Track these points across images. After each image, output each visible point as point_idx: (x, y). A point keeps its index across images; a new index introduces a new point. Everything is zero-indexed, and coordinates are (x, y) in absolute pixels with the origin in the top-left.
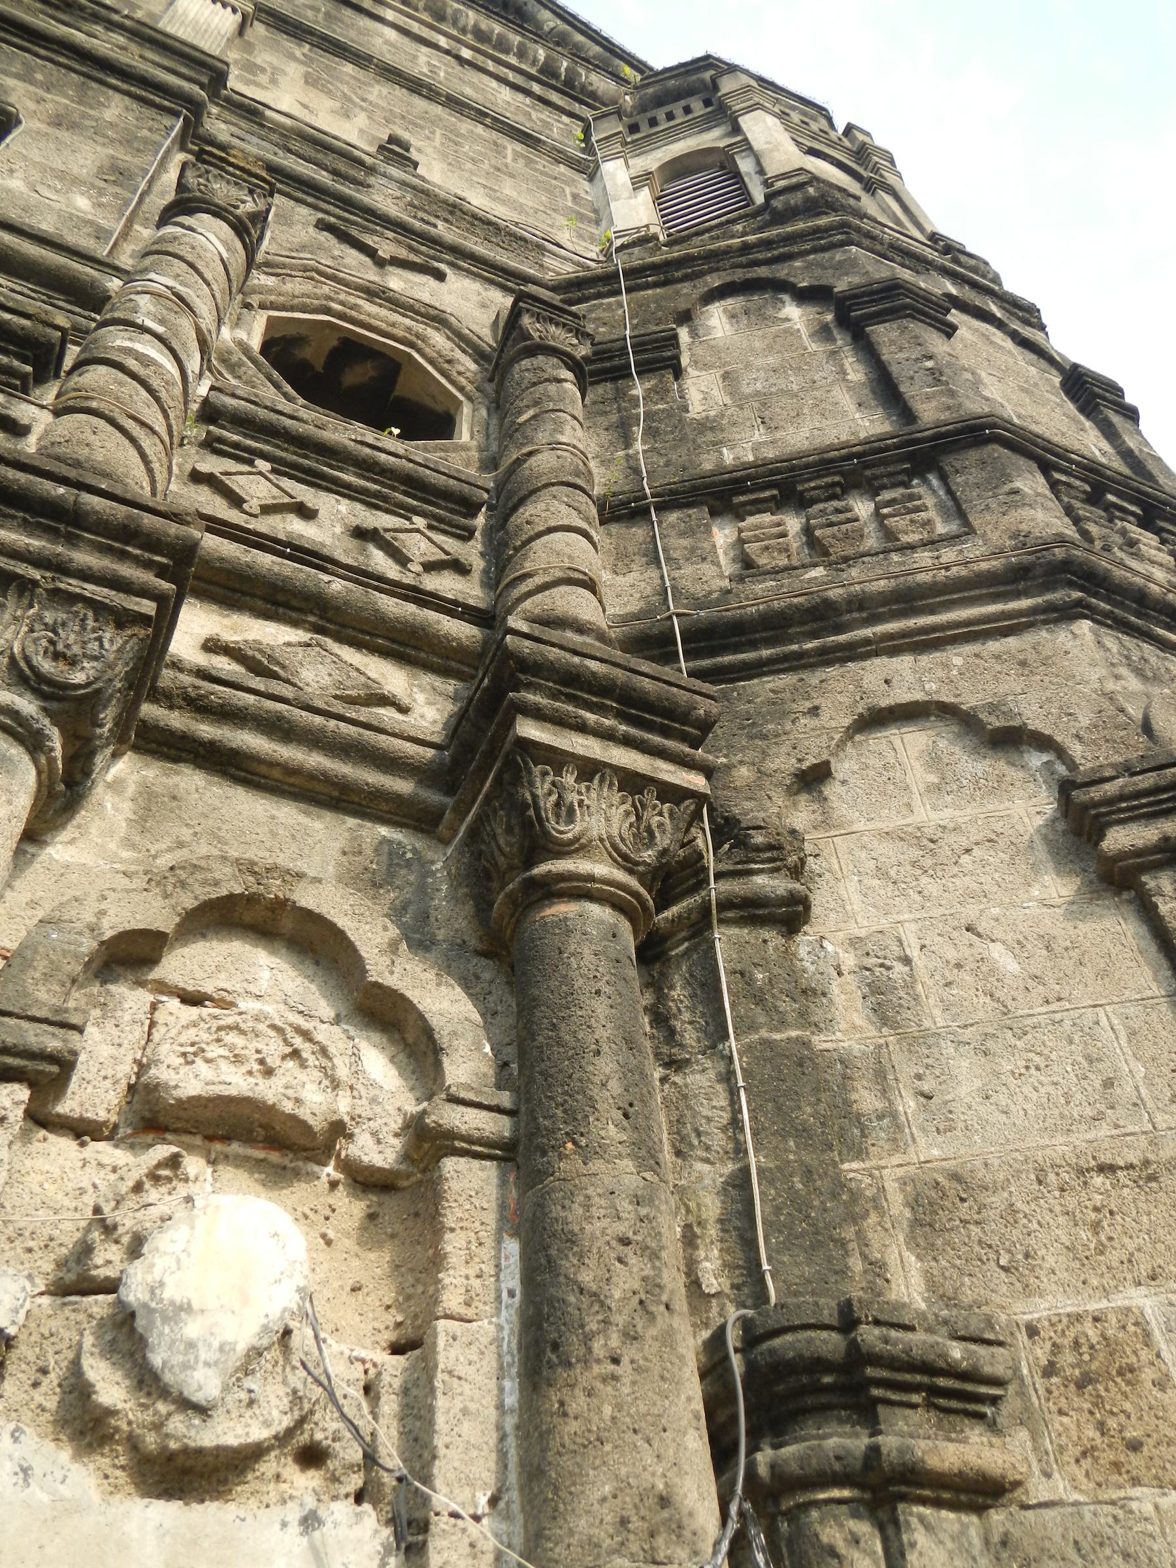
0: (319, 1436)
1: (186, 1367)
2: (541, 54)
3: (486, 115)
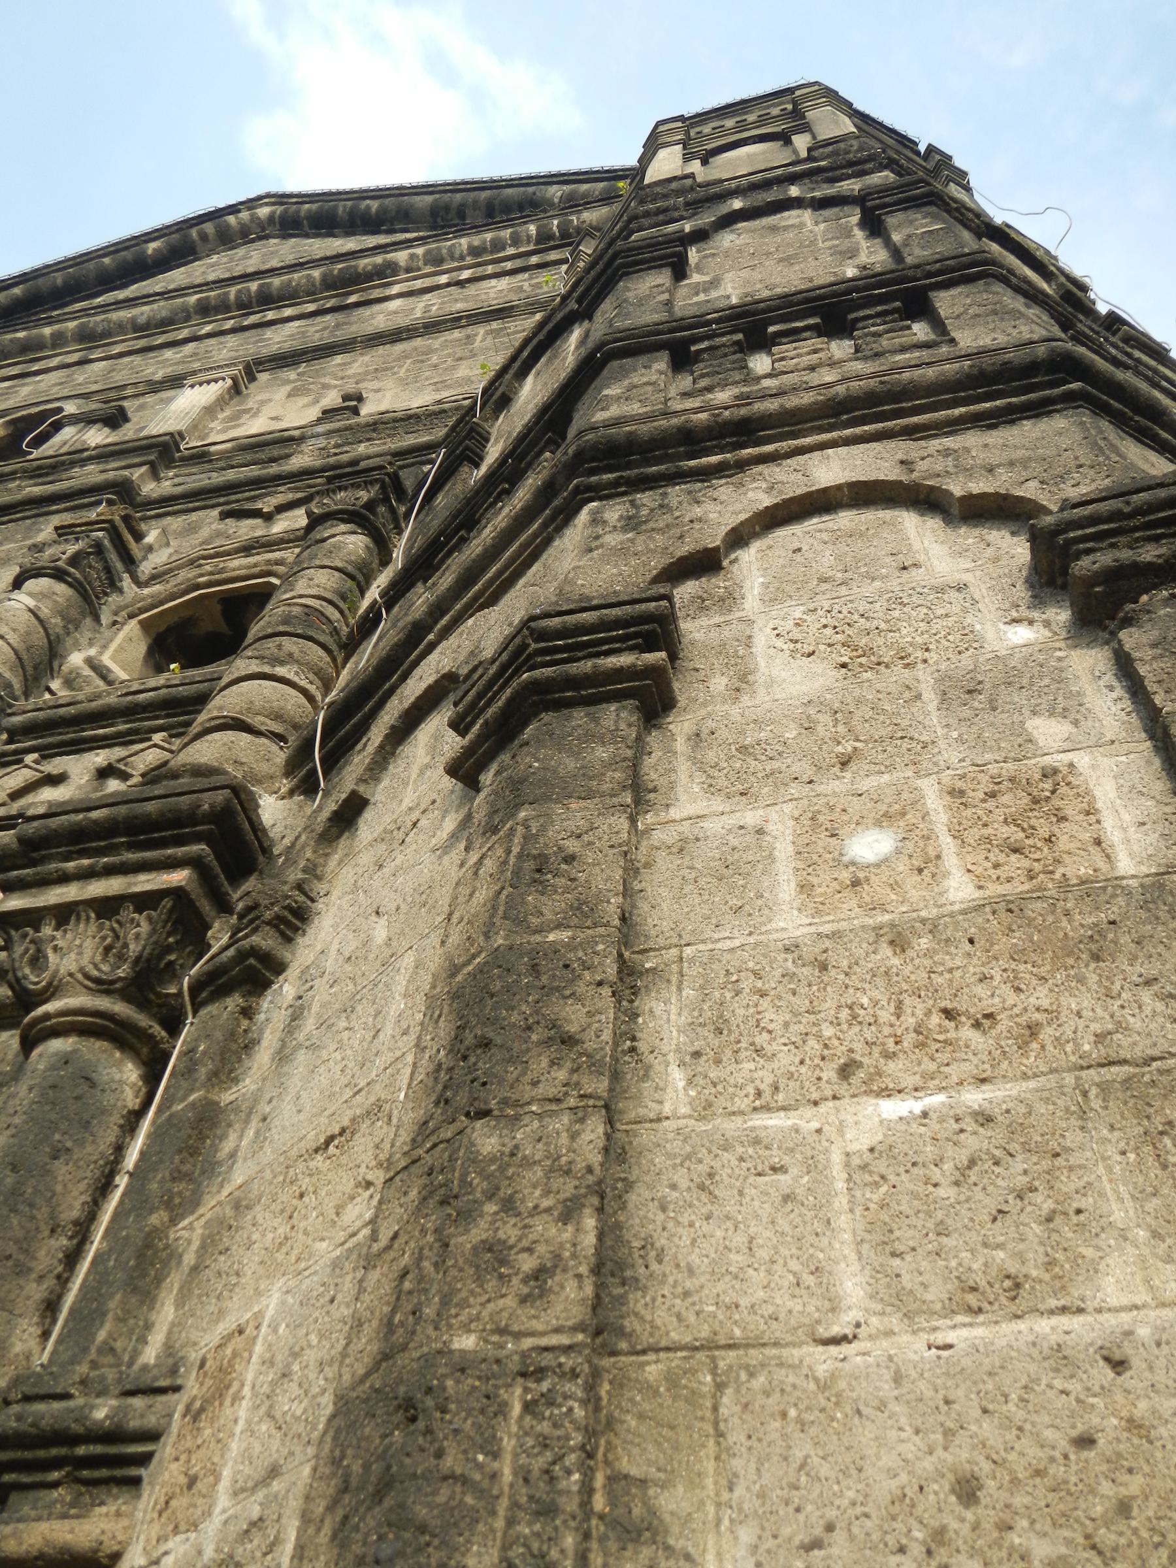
2: (532, 229)
3: (460, 318)
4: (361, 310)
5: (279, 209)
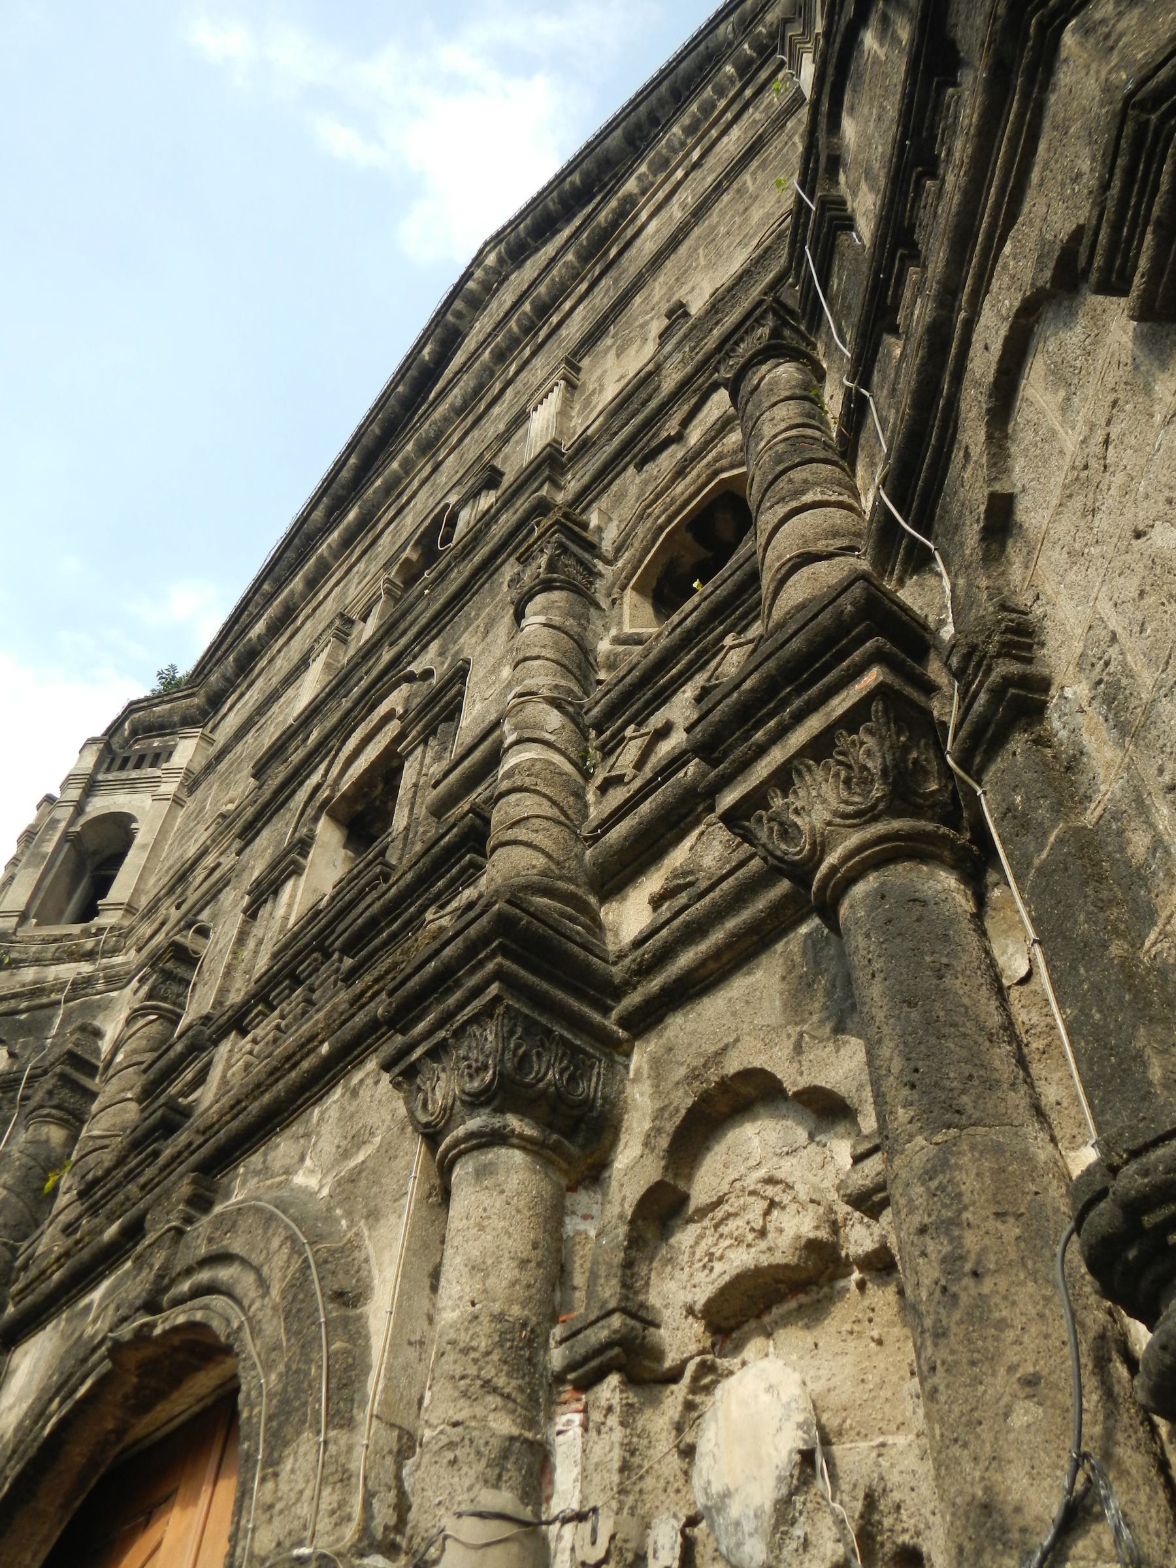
0: (905, 1538)
1: (739, 1545)
2: (729, 69)
3: (720, 183)
4: (626, 255)
5: (502, 247)
